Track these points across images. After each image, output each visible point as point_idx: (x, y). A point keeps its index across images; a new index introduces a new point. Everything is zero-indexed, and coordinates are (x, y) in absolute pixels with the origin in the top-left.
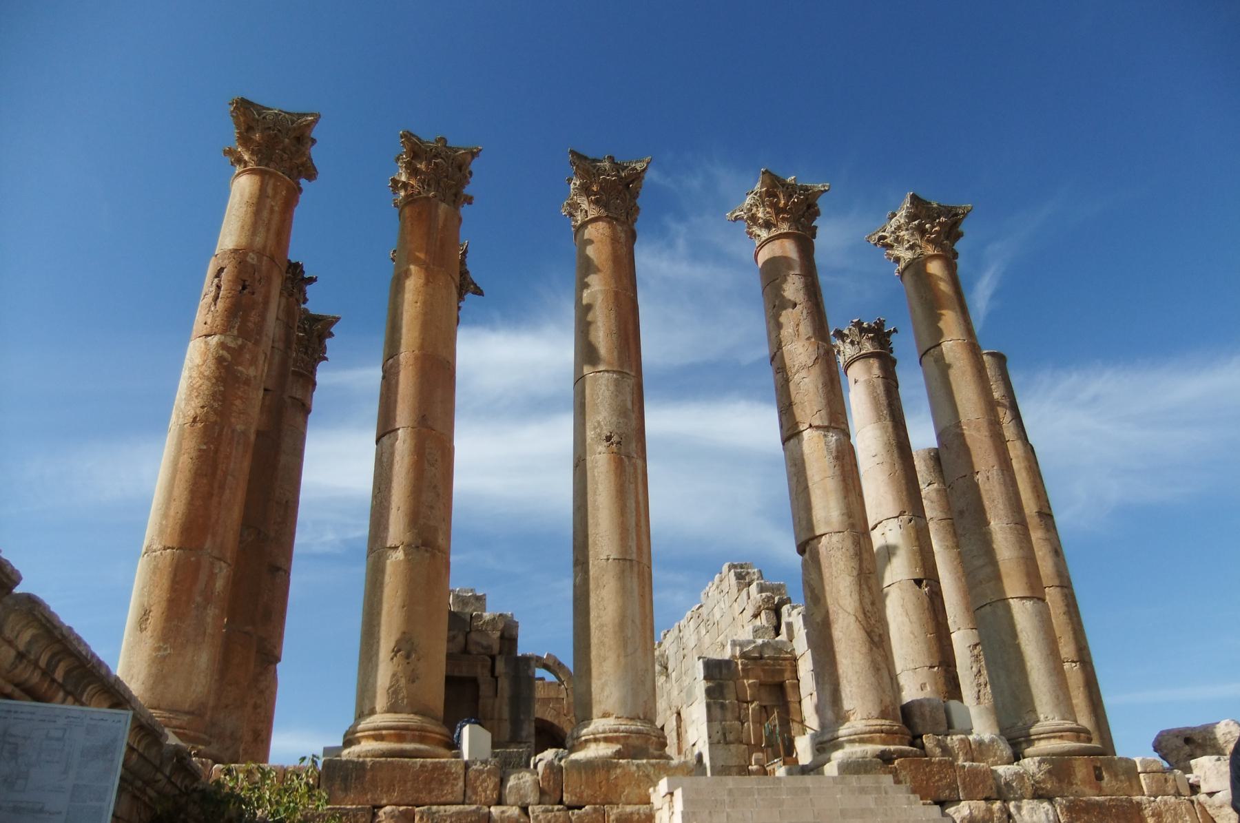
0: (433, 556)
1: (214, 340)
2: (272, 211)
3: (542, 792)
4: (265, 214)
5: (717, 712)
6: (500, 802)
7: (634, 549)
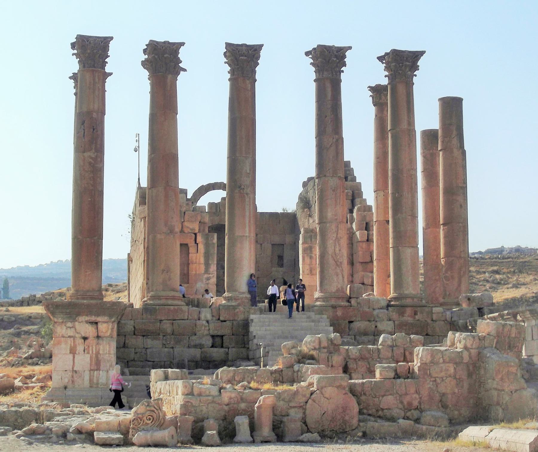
0: (174, 235)
1: (86, 154)
2: (99, 89)
3: (213, 316)
4: (97, 92)
5: (308, 260)
6: (199, 320)
7: (248, 231)
